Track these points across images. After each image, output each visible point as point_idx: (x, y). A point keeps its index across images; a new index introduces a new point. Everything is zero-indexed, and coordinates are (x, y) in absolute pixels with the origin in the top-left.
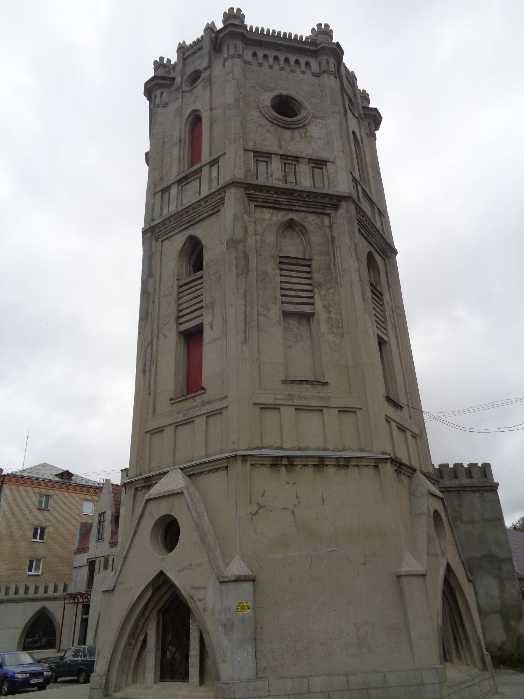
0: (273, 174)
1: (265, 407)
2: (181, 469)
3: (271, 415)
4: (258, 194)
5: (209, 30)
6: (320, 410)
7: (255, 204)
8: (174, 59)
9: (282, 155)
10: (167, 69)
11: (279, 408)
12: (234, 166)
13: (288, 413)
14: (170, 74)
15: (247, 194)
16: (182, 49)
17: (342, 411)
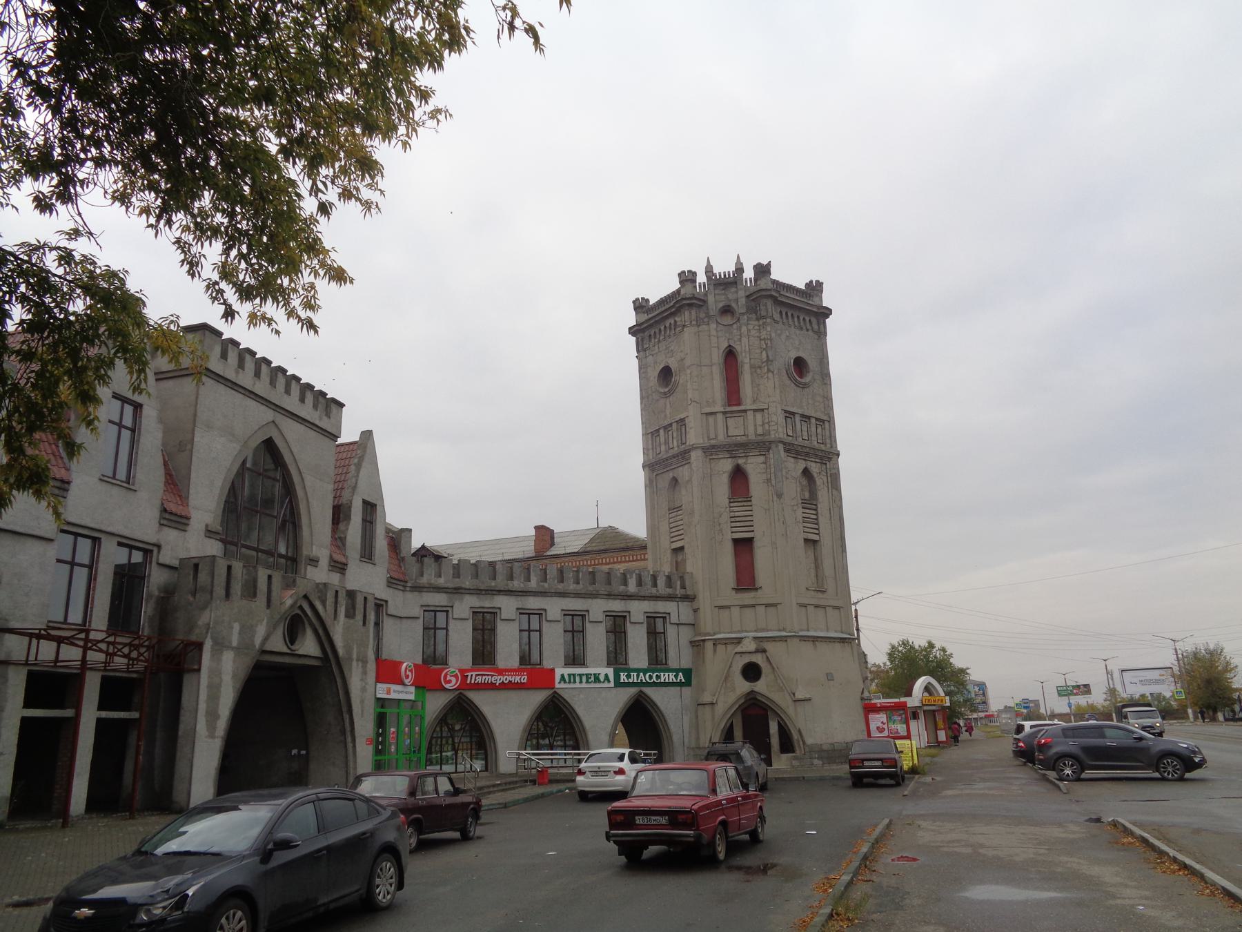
1: (801, 605)
4: (793, 451)
6: (824, 607)
8: (701, 278)
13: (811, 609)
17: (835, 608)
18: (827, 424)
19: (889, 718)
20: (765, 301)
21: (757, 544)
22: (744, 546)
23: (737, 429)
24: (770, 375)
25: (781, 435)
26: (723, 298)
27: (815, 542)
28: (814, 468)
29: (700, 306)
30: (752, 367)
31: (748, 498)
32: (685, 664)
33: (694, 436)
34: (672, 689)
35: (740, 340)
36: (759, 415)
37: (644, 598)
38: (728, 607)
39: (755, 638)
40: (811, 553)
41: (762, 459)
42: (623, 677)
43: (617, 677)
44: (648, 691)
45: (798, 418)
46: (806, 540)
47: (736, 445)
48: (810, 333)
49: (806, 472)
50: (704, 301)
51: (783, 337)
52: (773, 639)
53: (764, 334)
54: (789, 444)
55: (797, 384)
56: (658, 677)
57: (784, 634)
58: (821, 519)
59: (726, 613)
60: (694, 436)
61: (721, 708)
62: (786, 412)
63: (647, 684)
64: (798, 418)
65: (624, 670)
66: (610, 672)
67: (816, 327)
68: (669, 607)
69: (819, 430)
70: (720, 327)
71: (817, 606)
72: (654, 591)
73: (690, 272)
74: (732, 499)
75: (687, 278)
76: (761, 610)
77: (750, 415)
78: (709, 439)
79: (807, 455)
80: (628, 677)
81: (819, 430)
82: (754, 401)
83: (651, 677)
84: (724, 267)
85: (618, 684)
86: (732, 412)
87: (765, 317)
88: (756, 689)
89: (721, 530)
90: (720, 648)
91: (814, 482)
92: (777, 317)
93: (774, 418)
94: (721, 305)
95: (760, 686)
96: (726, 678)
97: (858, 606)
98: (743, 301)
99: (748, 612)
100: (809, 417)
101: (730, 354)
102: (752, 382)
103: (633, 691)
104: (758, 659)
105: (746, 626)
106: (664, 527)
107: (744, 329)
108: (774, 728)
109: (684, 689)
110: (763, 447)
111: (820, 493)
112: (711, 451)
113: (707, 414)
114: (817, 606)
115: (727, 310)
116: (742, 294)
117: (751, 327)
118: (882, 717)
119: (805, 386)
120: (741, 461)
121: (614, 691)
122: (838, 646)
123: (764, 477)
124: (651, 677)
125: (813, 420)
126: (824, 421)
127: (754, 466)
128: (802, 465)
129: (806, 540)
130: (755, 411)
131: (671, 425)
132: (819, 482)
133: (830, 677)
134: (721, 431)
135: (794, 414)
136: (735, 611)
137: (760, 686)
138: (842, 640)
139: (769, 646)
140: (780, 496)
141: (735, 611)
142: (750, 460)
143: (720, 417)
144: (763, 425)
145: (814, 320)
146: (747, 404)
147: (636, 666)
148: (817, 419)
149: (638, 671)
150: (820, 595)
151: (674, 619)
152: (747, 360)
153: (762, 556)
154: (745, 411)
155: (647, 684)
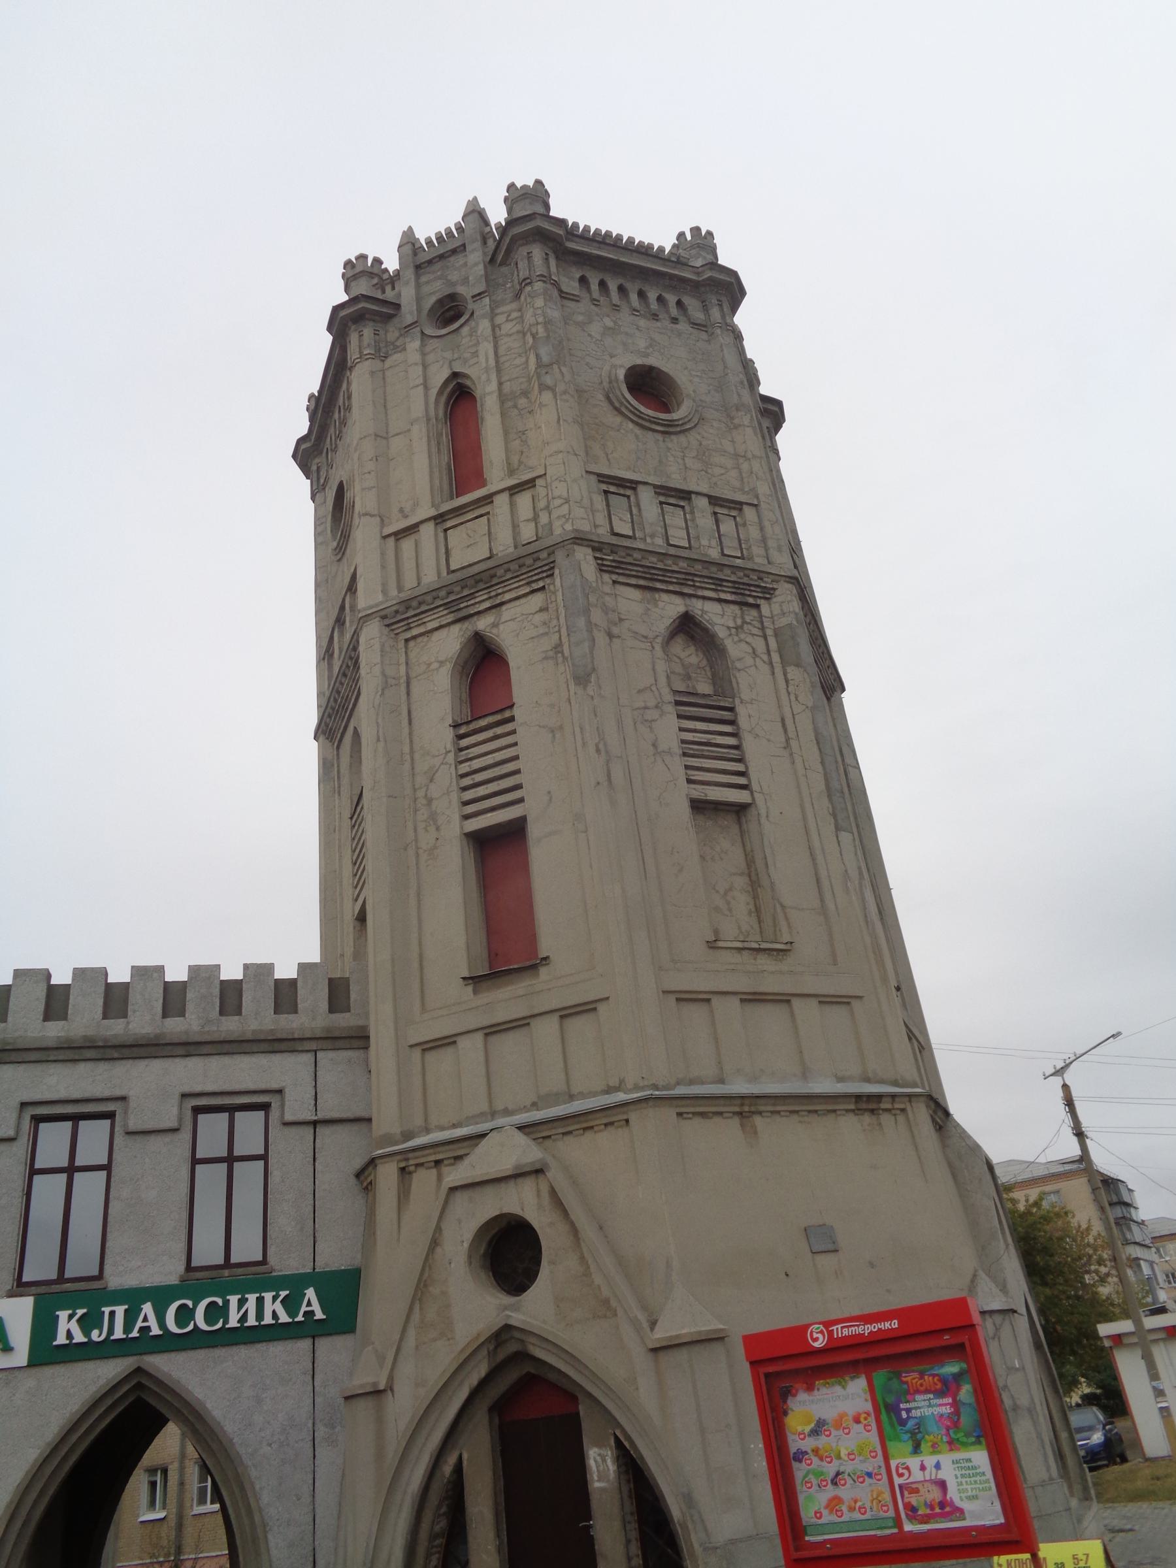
0: (652, 524)
1: (685, 998)
2: (521, 1128)
3: (696, 1013)
4: (619, 561)
5: (476, 215)
6: (784, 999)
7: (614, 577)
8: (392, 263)
9: (655, 486)
10: (375, 281)
11: (708, 1000)
12: (569, 503)
14: (384, 292)
15: (596, 558)
16: (408, 242)
17: (826, 1000)
18: (749, 512)
19: (888, 1413)
20: (523, 251)
21: (534, 831)
22: (498, 848)
23: (469, 547)
24: (547, 397)
25: (585, 527)
26: (438, 284)
27: (740, 810)
28: (717, 616)
29: (388, 318)
30: (503, 398)
31: (504, 712)
32: (334, 1255)
33: (369, 597)
34: (277, 1350)
35: (475, 354)
36: (524, 500)
37: (189, 1048)
38: (448, 1041)
39: (521, 1128)
40: (727, 844)
41: (537, 600)
42: (67, 1327)
43: (43, 1325)
44: (166, 1365)
45: (646, 497)
46: (699, 806)
47: (462, 583)
48: (683, 326)
49: (687, 627)
50: (397, 306)
51: (595, 329)
52: (582, 1122)
53: (529, 317)
54: (614, 549)
55: (643, 424)
56: (213, 1312)
57: (621, 1097)
58: (751, 746)
59: (441, 1061)
60: (369, 597)
61: (404, 1406)
62: (602, 478)
63: (168, 1343)
64: (646, 497)
65: (69, 1300)
66: (18, 1315)
67: (699, 316)
68: (286, 1072)
69: (727, 527)
70: (434, 343)
71: (753, 999)
72: (231, 1026)
73: (362, 257)
74: (461, 729)
75: (358, 271)
76: (547, 1029)
77: (502, 501)
78: (400, 589)
79: (687, 578)
80: (86, 1324)
81: (727, 527)
82: (511, 472)
83: (185, 1314)
84: (436, 219)
85: (45, 1351)
86: (457, 511)
87: (527, 282)
88: (516, 1319)
89: (433, 817)
90: (423, 1180)
91: (722, 652)
92: (571, 285)
93: (560, 489)
94: (433, 299)
95: (536, 1309)
96: (422, 1287)
97: (1070, 1077)
98: (480, 270)
99: (508, 1044)
100: (686, 495)
101: (459, 396)
102: (506, 433)
103: (110, 1371)
104: (524, 1202)
105: (480, 1091)
106: (348, 870)
107: (484, 326)
108: (600, 1465)
109: (323, 1344)
110: (532, 567)
111: (743, 681)
112: (404, 617)
113: (399, 535)
114: (753, 999)
115: (449, 311)
116: (475, 257)
117: (500, 319)
118: (849, 1397)
119: (670, 429)
120: (482, 624)
121: (29, 1381)
122: (850, 1126)
123: (547, 644)
124: (185, 1314)
125: (703, 503)
126: (738, 506)
127: (517, 629)
128: (671, 607)
129: (699, 806)
130: (514, 490)
131: (342, 608)
132: (735, 649)
133: (821, 1240)
134: (424, 564)
135: (633, 485)
136: (472, 1047)
137: (536, 1309)
138: (868, 1104)
139: (576, 1151)
140: (582, 680)
141: (472, 1047)
142: (507, 612)
143: (428, 530)
144: (535, 519)
145: (690, 302)
146: (496, 478)
147: (131, 1281)
148: (714, 500)
149: (133, 1298)
150: (764, 962)
151: (297, 1106)
152: (493, 386)
153: (554, 868)
154: (488, 499)
155: (168, 1343)
